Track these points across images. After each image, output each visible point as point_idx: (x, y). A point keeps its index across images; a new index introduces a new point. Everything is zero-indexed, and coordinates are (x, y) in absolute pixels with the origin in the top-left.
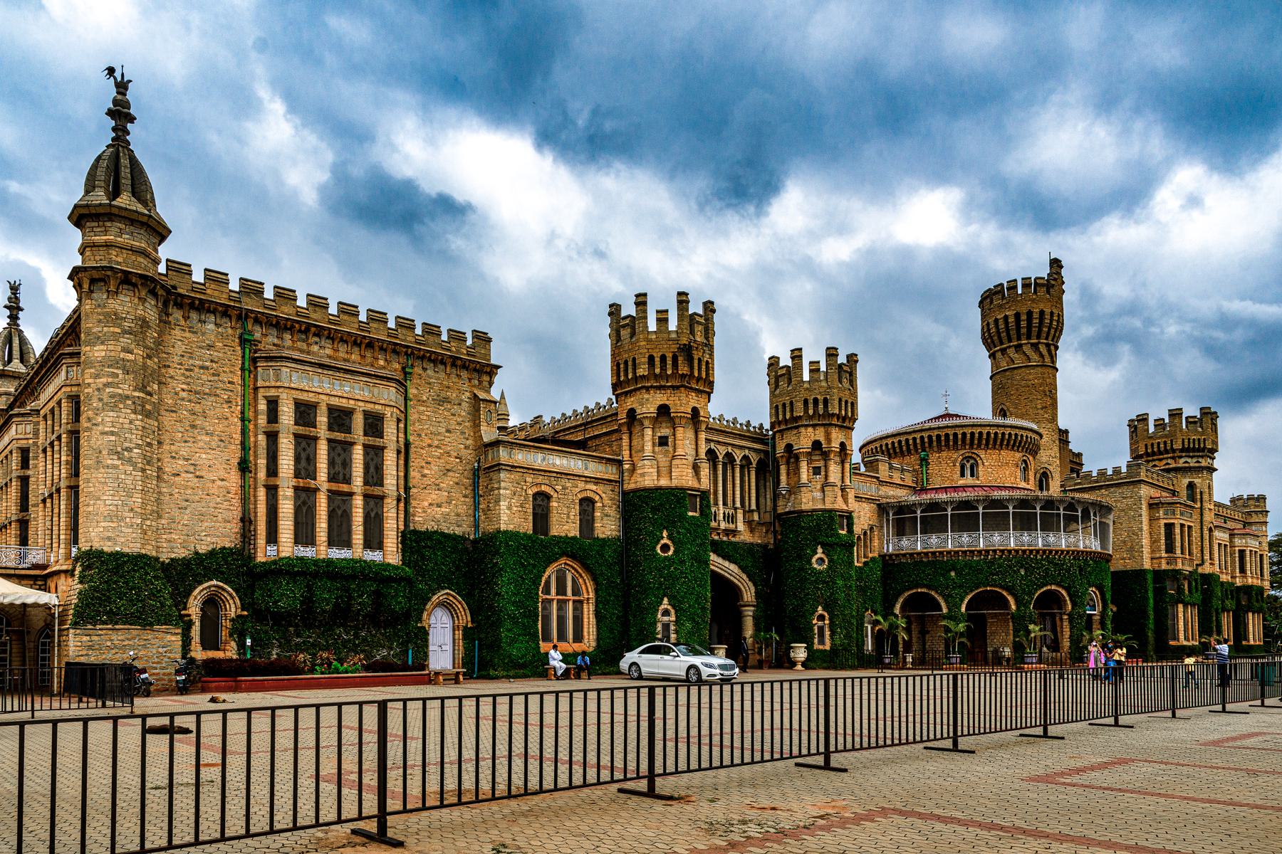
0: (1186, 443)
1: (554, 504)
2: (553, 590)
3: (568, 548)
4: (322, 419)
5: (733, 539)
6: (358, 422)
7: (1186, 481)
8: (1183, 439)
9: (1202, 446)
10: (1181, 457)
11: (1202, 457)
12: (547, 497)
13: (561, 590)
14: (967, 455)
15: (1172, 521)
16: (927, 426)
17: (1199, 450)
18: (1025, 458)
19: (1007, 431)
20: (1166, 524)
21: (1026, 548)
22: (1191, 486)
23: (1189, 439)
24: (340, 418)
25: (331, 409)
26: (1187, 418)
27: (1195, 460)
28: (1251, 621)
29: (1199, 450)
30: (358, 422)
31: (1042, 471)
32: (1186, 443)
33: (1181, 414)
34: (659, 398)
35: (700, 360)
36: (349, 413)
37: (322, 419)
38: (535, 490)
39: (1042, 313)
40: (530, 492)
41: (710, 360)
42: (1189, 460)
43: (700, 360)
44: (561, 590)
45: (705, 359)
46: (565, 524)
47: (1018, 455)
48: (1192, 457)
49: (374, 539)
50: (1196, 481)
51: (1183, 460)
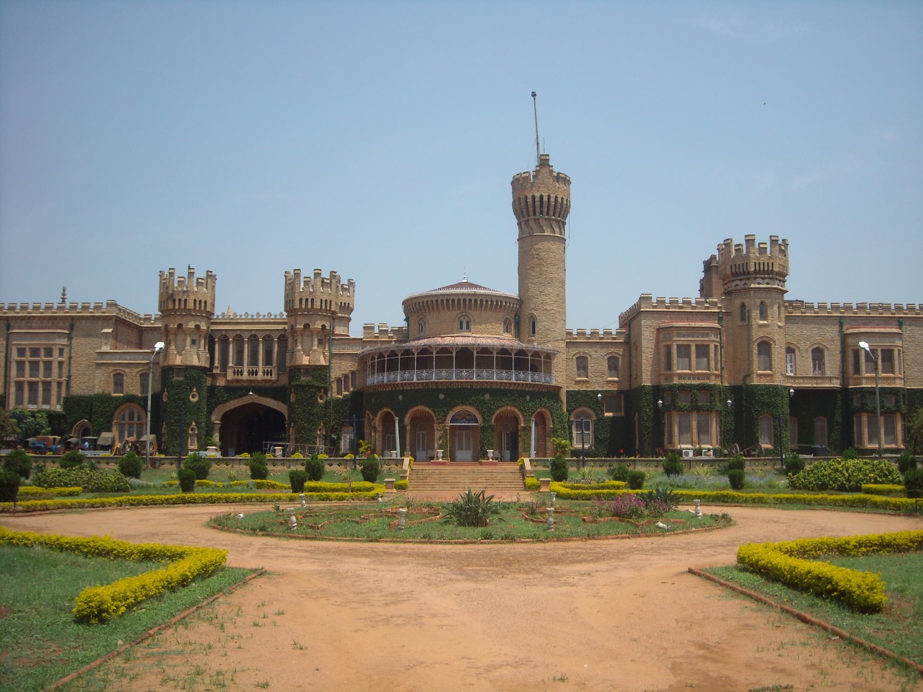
0: (734, 269)
1: (125, 378)
2: (127, 418)
3: (130, 399)
4: (28, 353)
5: (275, 385)
6: (42, 352)
7: (737, 302)
8: (731, 266)
9: (745, 269)
10: (733, 281)
11: (748, 279)
12: (123, 375)
13: (131, 417)
14: (421, 317)
15: (669, 343)
16: (435, 293)
17: (744, 273)
18: (464, 314)
19: (417, 301)
20: (665, 346)
21: (424, 381)
22: (743, 305)
23: (736, 265)
24: (35, 352)
25: (31, 349)
26: (760, 244)
27: (743, 282)
28: (855, 422)
29: (744, 273)
30: (42, 352)
31: (530, 316)
32: (734, 269)
33: (754, 240)
34: (179, 320)
35: (180, 300)
36: (38, 349)
37: (28, 353)
38: (114, 373)
39: (534, 197)
40: (112, 374)
41: (187, 299)
42: (739, 282)
43: (180, 300)
44: (131, 417)
45: (184, 299)
46: (133, 387)
47: (454, 313)
48: (741, 280)
49: (47, 401)
50: (746, 301)
51: (734, 284)
